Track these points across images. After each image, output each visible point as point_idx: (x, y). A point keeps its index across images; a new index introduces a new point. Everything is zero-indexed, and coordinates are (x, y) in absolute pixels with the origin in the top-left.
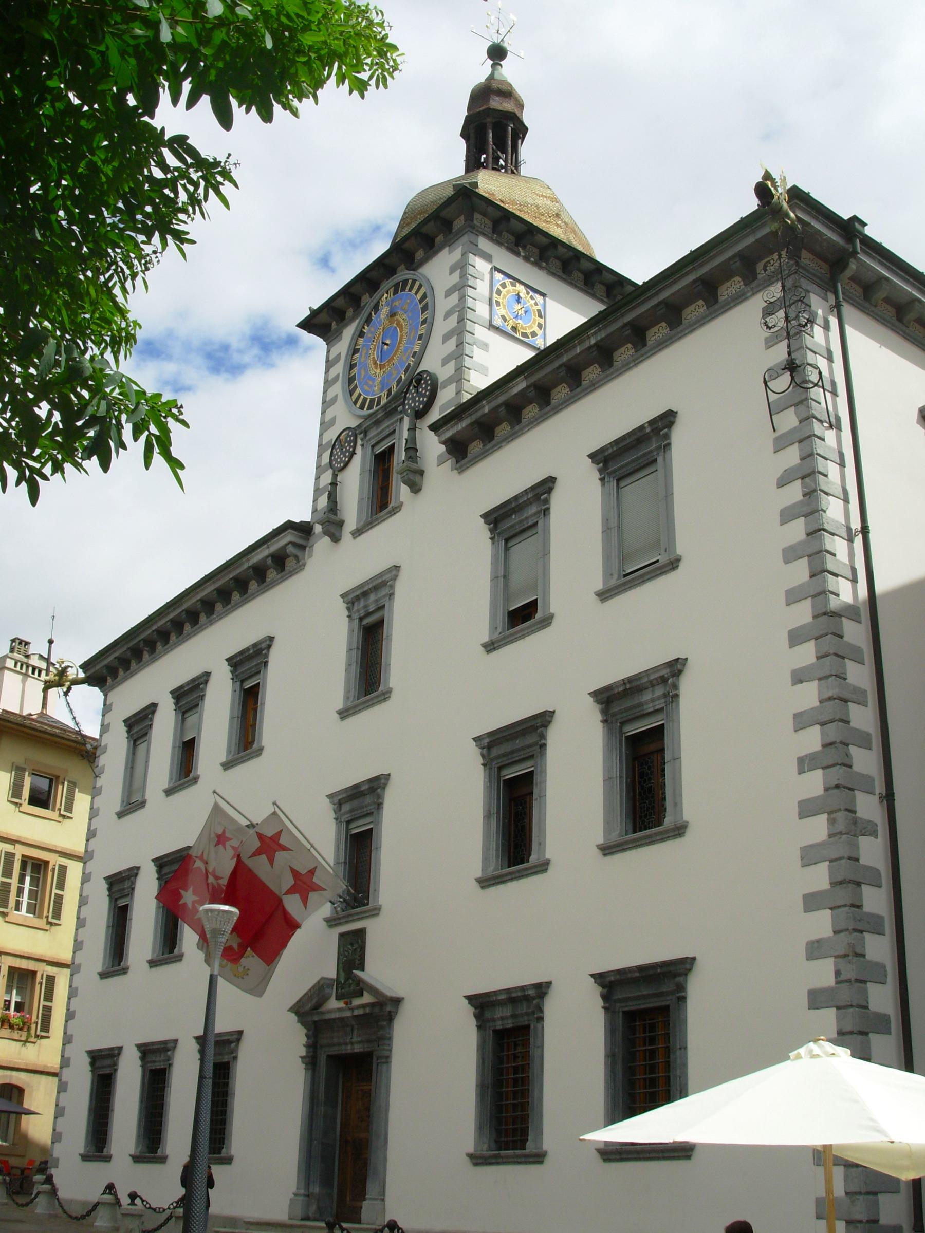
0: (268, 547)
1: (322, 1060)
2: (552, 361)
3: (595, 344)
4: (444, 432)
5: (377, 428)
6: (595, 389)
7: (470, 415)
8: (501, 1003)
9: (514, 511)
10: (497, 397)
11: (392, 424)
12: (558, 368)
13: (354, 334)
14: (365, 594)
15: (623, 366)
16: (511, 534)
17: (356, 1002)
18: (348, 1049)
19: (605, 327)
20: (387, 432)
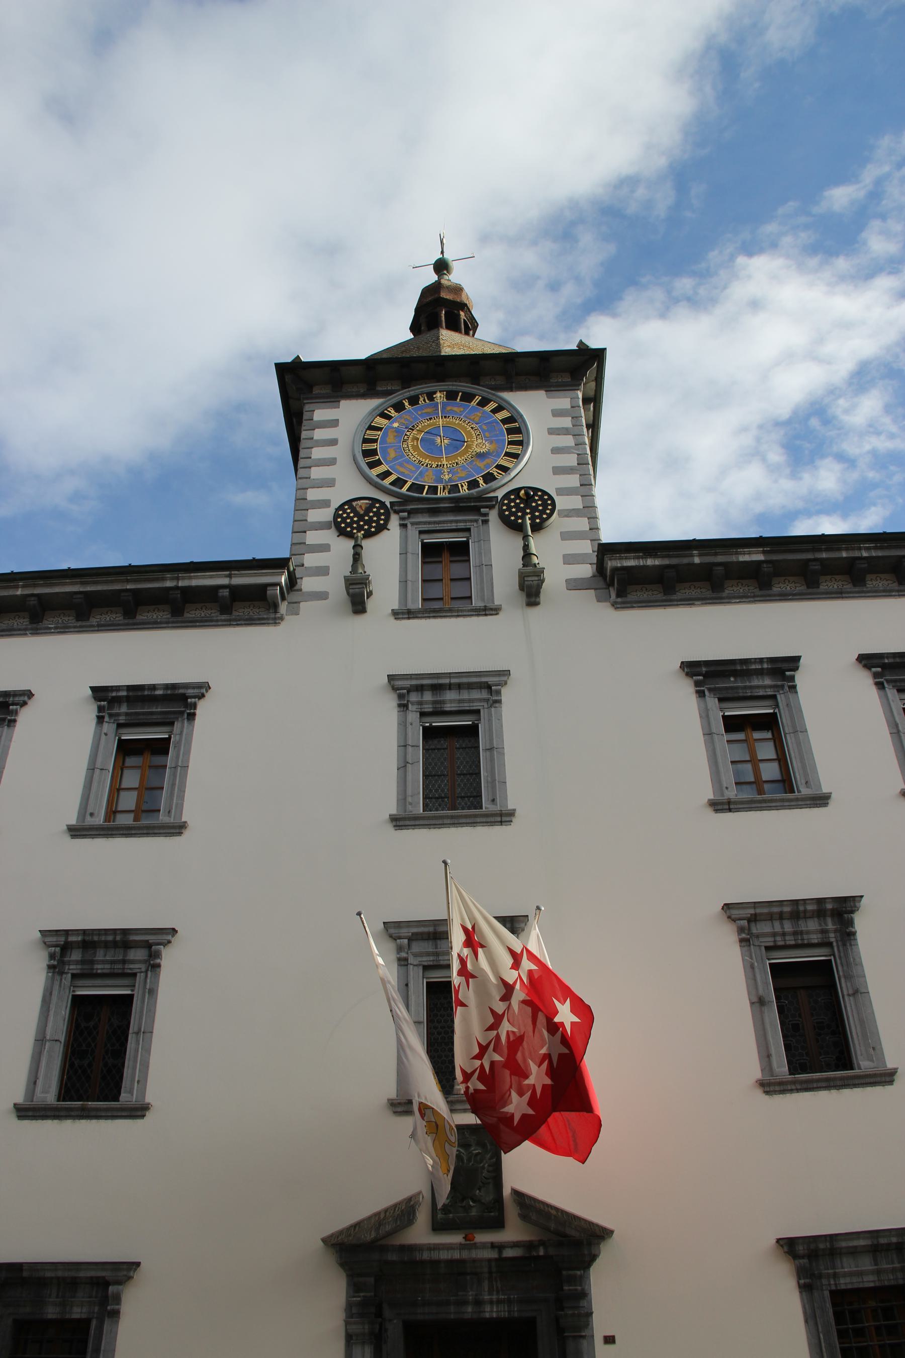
0: (230, 576)
1: (394, 1331)
2: (807, 551)
3: (865, 558)
4: (626, 558)
5: (430, 516)
6: (843, 598)
7: (669, 556)
8: (854, 1252)
9: (736, 674)
10: (716, 554)
11: (471, 521)
12: (810, 560)
13: (374, 410)
14: (437, 688)
15: (884, 591)
16: (730, 695)
17: (482, 1237)
18: (452, 1313)
19: (881, 548)
20: (461, 525)
